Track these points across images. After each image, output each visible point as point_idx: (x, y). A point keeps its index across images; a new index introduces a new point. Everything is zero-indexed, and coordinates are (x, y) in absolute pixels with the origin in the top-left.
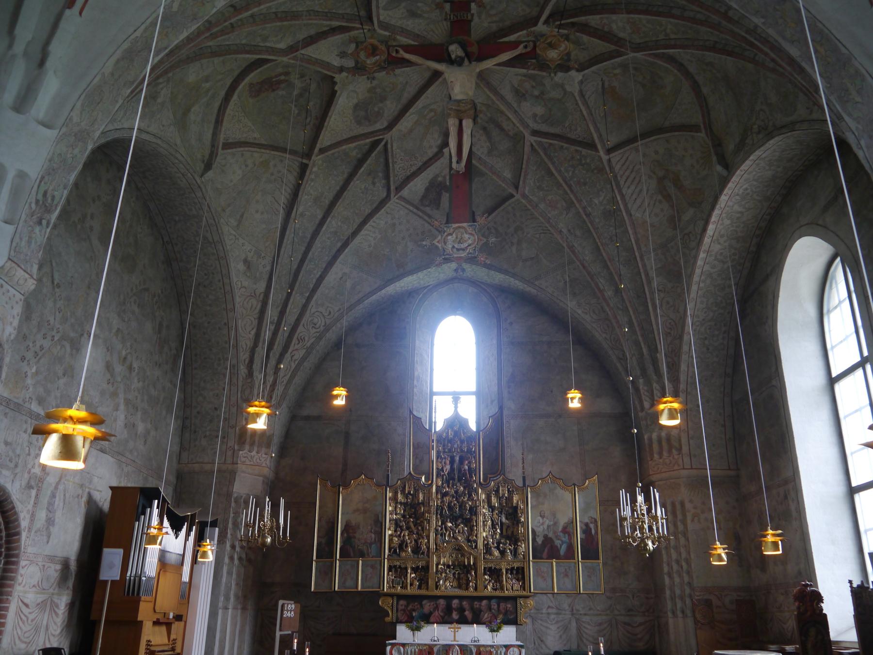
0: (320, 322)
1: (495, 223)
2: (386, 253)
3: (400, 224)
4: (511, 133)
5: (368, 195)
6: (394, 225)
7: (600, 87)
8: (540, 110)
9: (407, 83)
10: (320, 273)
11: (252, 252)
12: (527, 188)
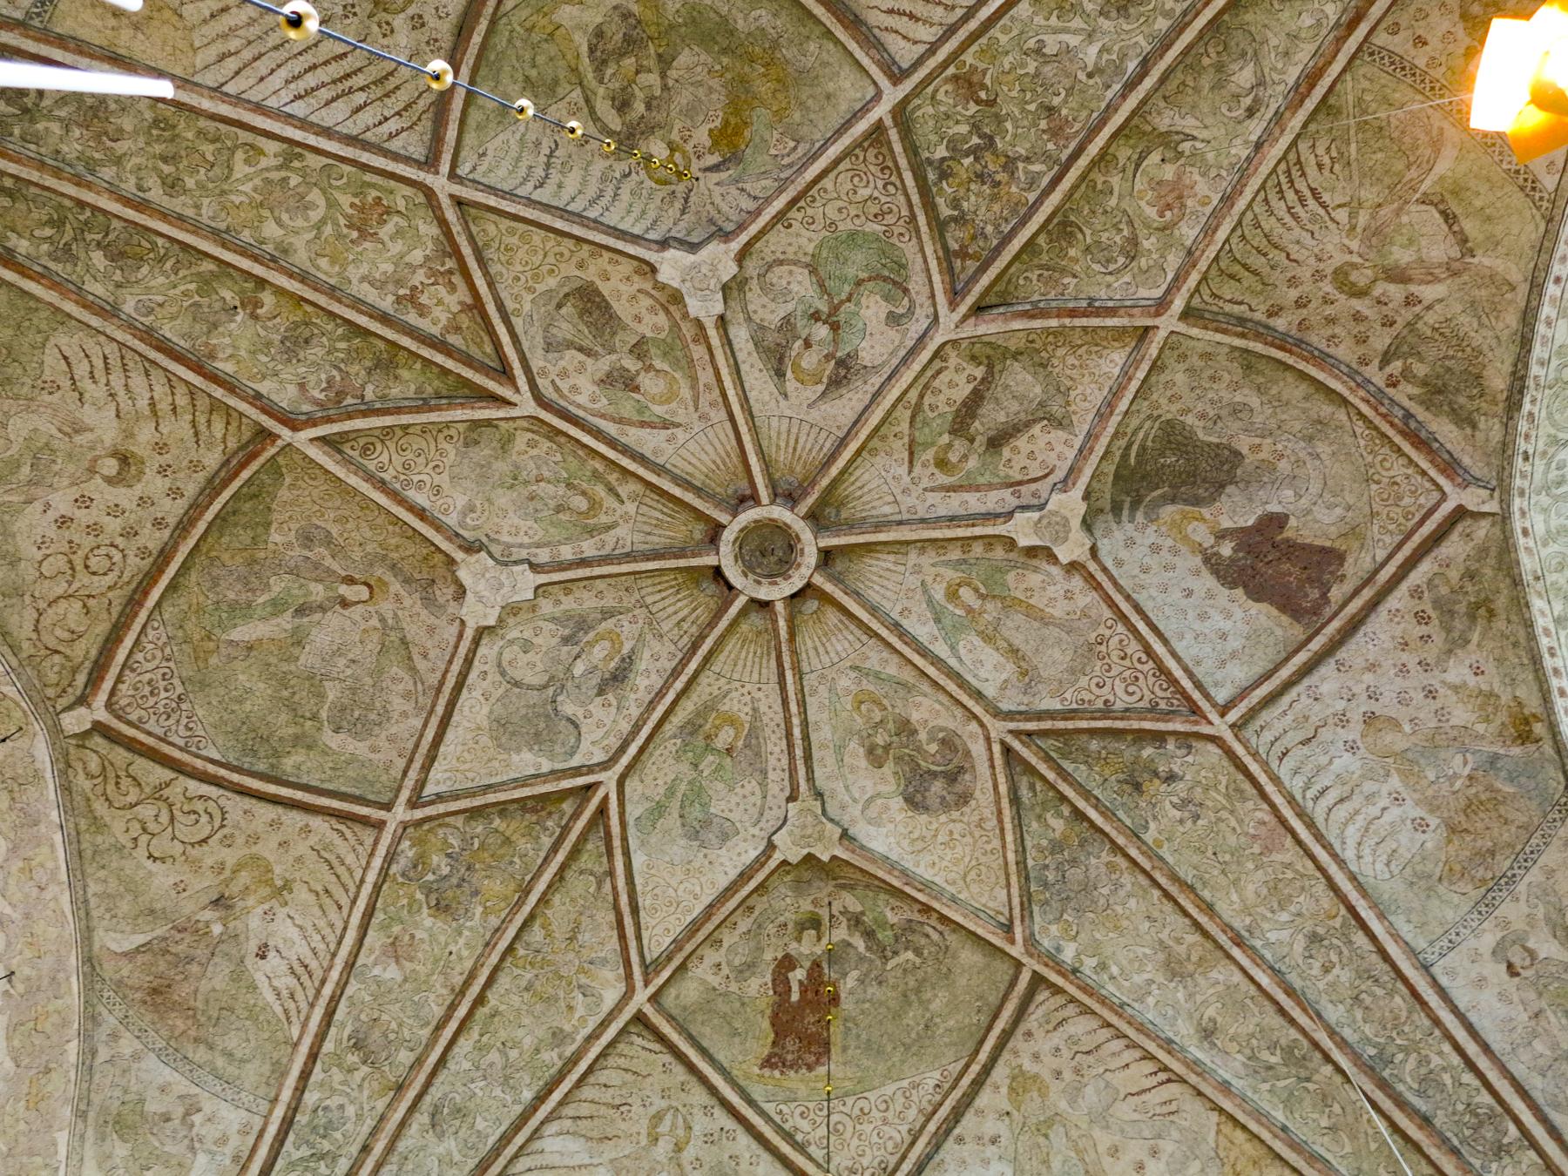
1: (1364, 361)
2: (1467, 771)
3: (1373, 696)
4: (979, 372)
5: (1210, 804)
6: (1370, 719)
7: (724, 175)
8: (873, 309)
9: (855, 668)
12: (1143, 292)
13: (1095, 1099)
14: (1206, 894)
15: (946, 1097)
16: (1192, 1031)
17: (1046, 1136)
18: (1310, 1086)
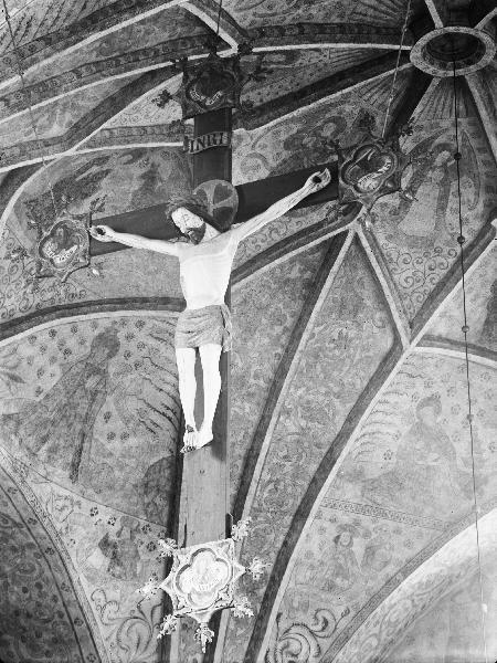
0: (305, 649)
10: (282, 538)
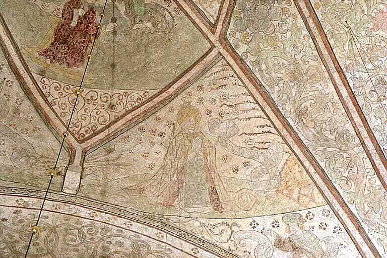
11: (283, 226)
13: (224, 130)
14: (332, 42)
15: (143, 104)
16: (292, 110)
17: (190, 141)
18: (345, 155)
